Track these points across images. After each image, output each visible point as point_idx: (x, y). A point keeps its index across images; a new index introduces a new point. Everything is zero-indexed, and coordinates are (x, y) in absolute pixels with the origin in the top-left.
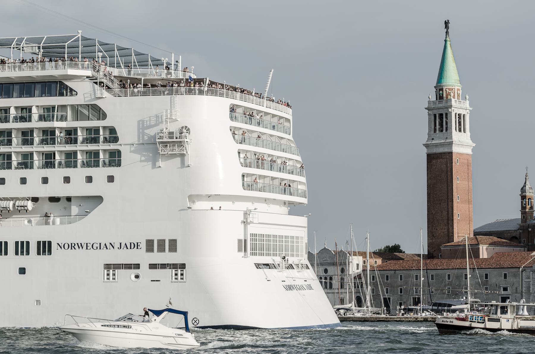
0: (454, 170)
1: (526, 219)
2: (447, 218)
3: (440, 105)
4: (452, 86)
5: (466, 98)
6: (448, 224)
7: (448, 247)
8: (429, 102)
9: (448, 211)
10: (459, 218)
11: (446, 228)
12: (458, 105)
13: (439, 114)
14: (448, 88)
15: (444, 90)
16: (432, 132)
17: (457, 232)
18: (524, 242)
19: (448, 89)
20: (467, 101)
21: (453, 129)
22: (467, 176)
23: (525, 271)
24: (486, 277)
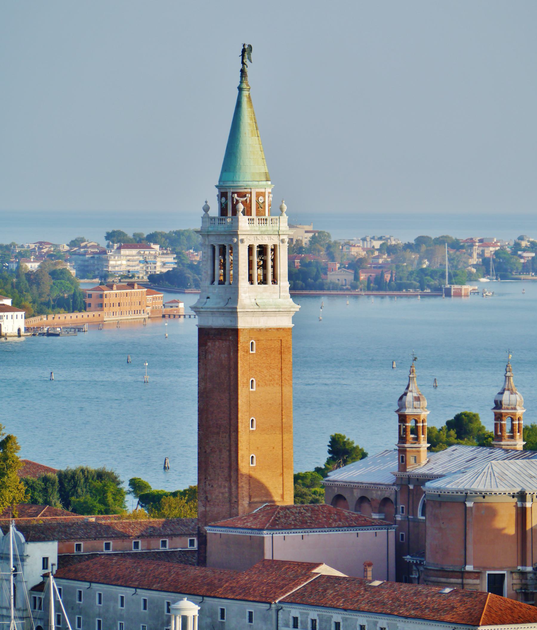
0: (242, 367)
1: (405, 465)
2: (228, 465)
3: (221, 228)
4: (245, 188)
5: (281, 209)
6: (230, 476)
7: (217, 529)
8: (206, 218)
9: (230, 451)
10: (254, 465)
11: (227, 485)
12: (257, 229)
13: (220, 245)
14: (236, 193)
15: (229, 195)
16: (208, 282)
17: (247, 494)
18: (403, 512)
19: (236, 195)
20: (285, 215)
21: (243, 279)
22: (280, 373)
23: (281, 611)
24: (223, 617)
